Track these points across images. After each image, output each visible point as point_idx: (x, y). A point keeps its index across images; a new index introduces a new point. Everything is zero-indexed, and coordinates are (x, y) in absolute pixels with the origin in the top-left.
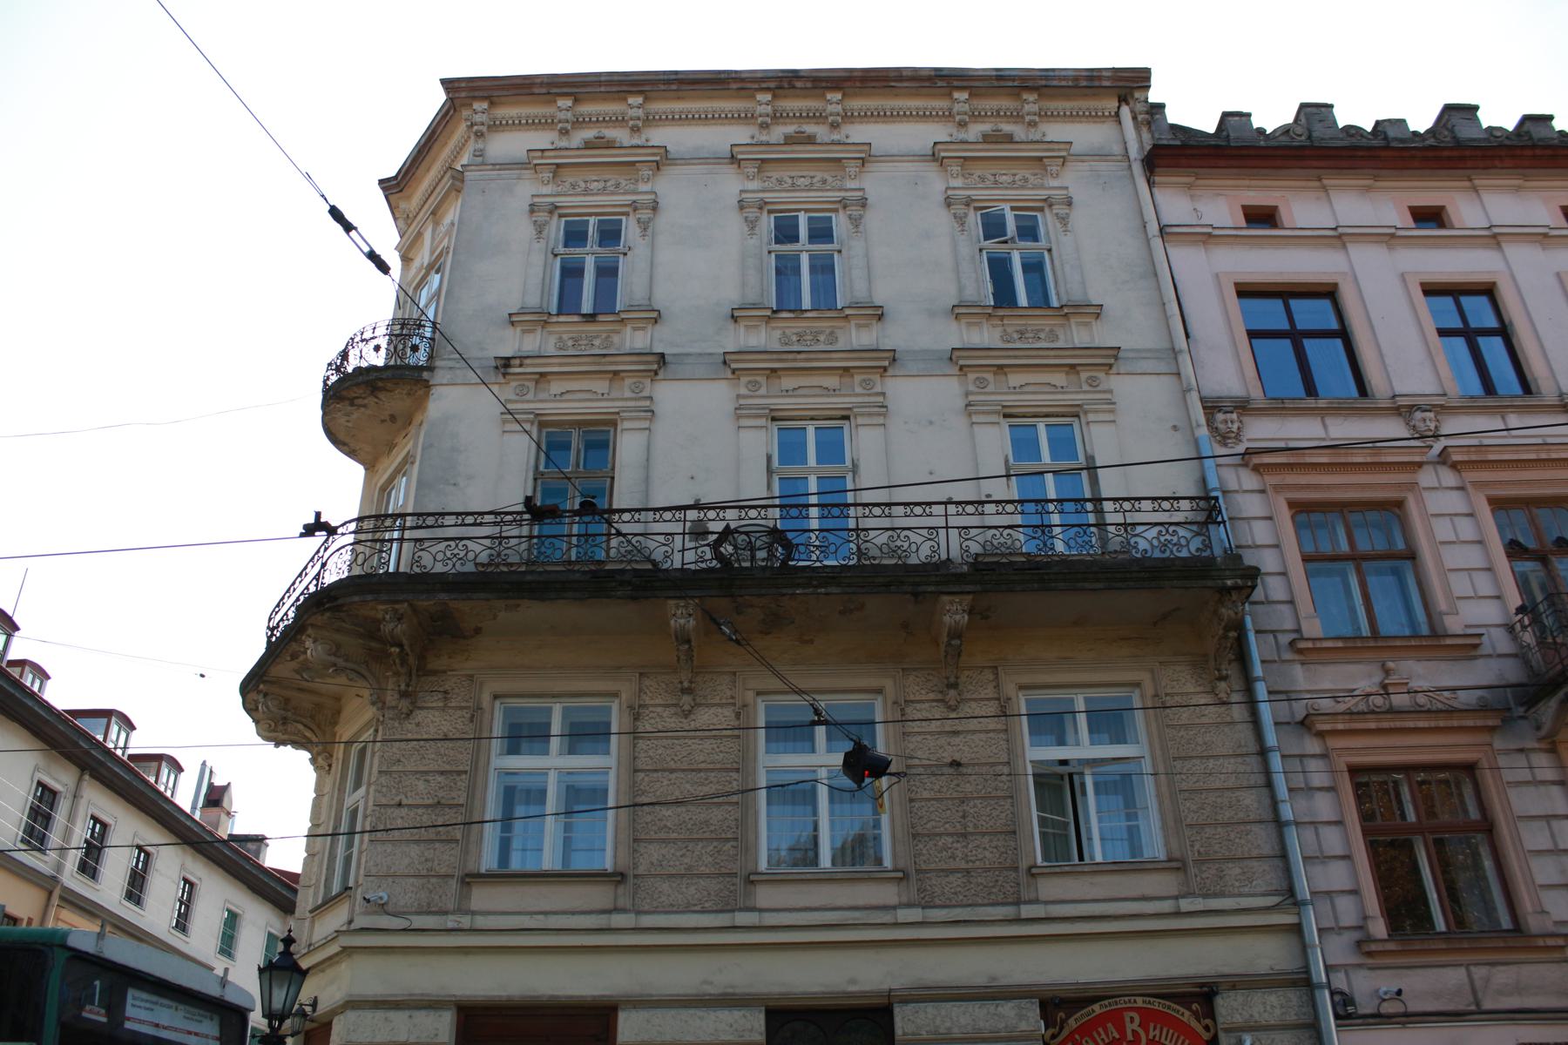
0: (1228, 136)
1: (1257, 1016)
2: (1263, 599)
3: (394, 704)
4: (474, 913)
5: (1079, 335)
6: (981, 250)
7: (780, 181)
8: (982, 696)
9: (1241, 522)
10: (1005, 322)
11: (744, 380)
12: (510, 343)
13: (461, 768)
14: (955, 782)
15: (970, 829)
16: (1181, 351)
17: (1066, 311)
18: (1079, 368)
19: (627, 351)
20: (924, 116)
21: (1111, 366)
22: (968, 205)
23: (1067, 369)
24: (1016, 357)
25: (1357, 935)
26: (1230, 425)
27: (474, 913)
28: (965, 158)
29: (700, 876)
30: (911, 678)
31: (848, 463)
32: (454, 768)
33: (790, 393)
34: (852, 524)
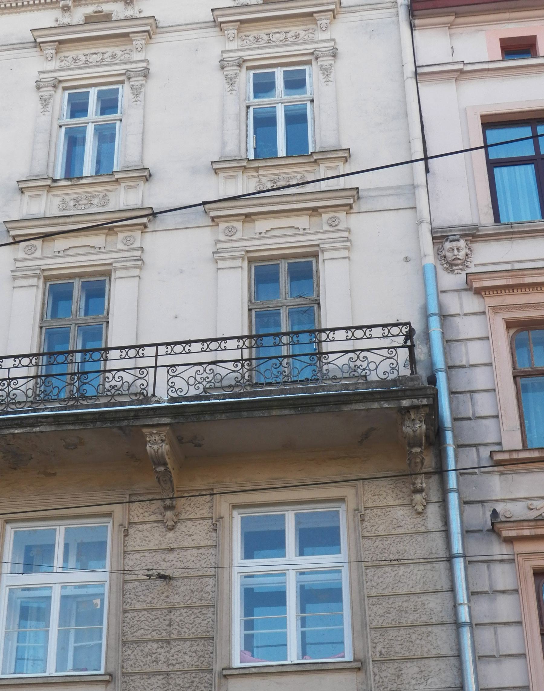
2: (470, 415)
6: (248, 107)
7: (75, 60)
8: (198, 516)
9: (459, 343)
10: (261, 173)
14: (166, 594)
15: (174, 636)
16: (418, 186)
17: (315, 157)
18: (320, 210)
21: (350, 206)
22: (239, 66)
23: (310, 212)
24: (261, 205)
26: (456, 252)
28: (242, 22)
33: (62, 253)
34: (75, 368)
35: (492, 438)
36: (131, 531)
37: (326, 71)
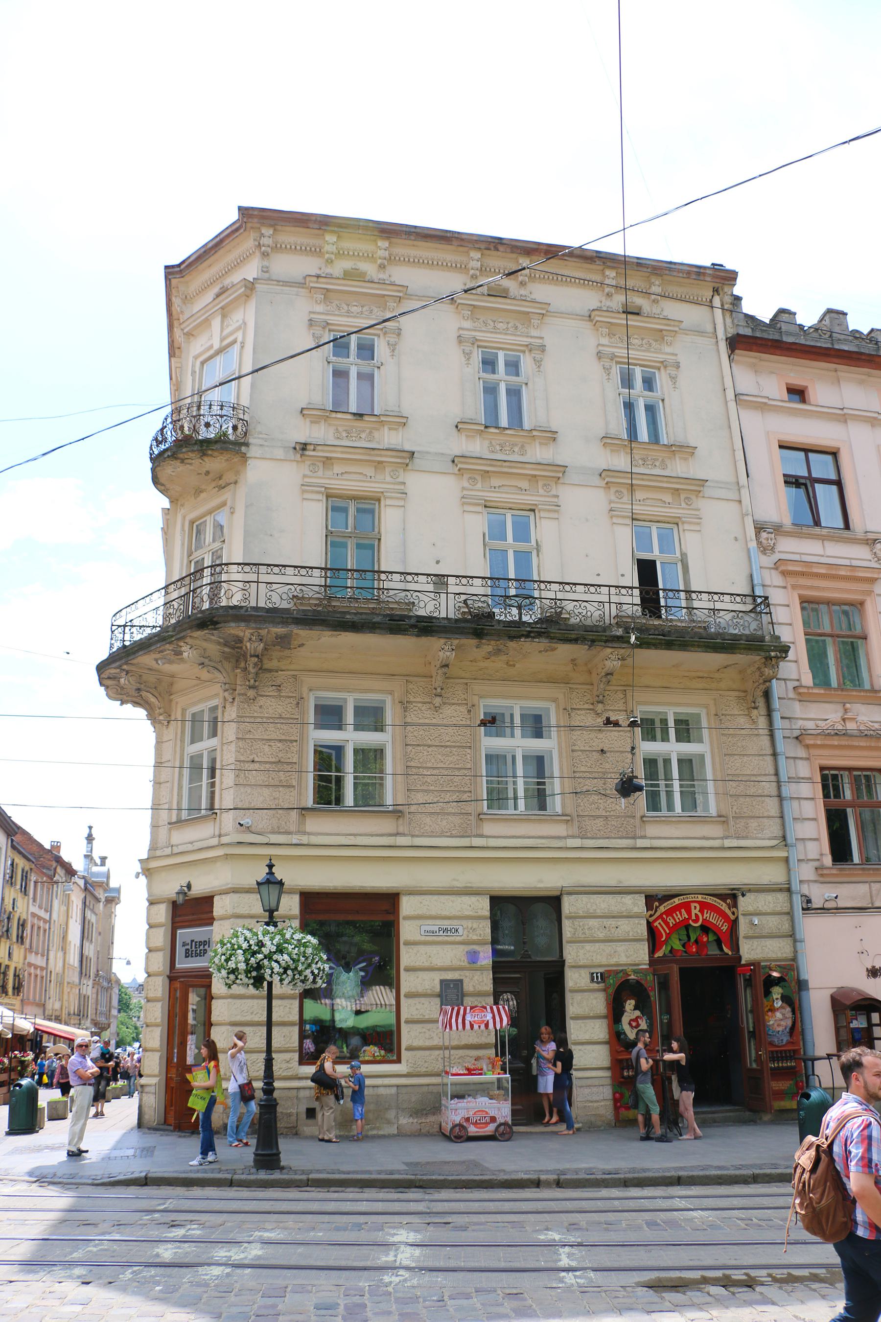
0: (780, 328)
1: (760, 908)
3: (242, 692)
4: (309, 834)
5: (679, 468)
11: (466, 476)
12: (302, 432)
13: (292, 738)
16: (743, 486)
19: (386, 446)
20: (584, 283)
22: (612, 360)
24: (643, 480)
25: (816, 864)
27: (309, 834)
29: (448, 814)
30: (575, 693)
31: (533, 543)
32: (288, 738)
35: (795, 677)
36: (573, 714)
37: (673, 379)
